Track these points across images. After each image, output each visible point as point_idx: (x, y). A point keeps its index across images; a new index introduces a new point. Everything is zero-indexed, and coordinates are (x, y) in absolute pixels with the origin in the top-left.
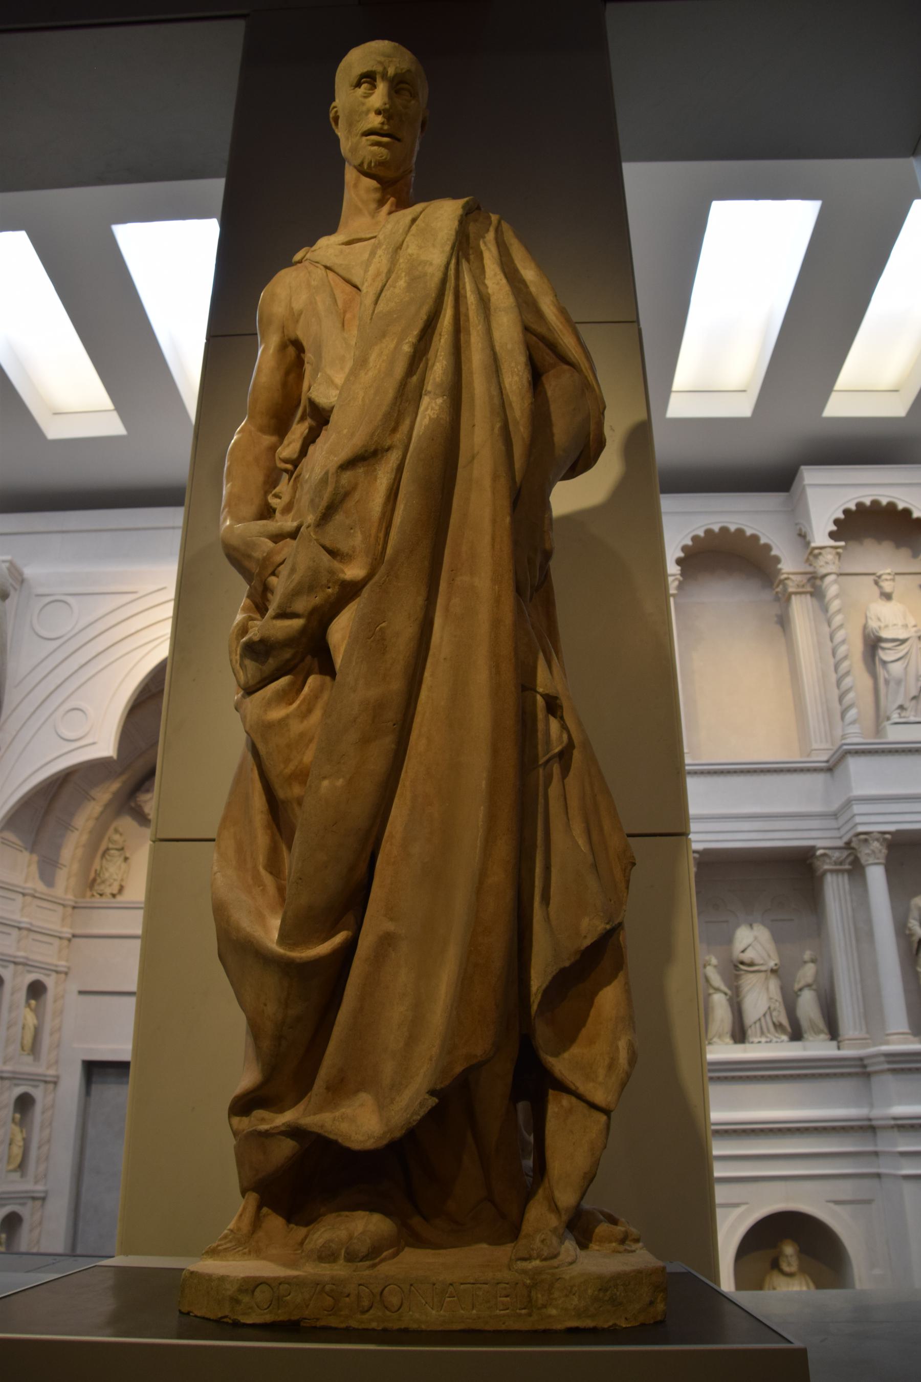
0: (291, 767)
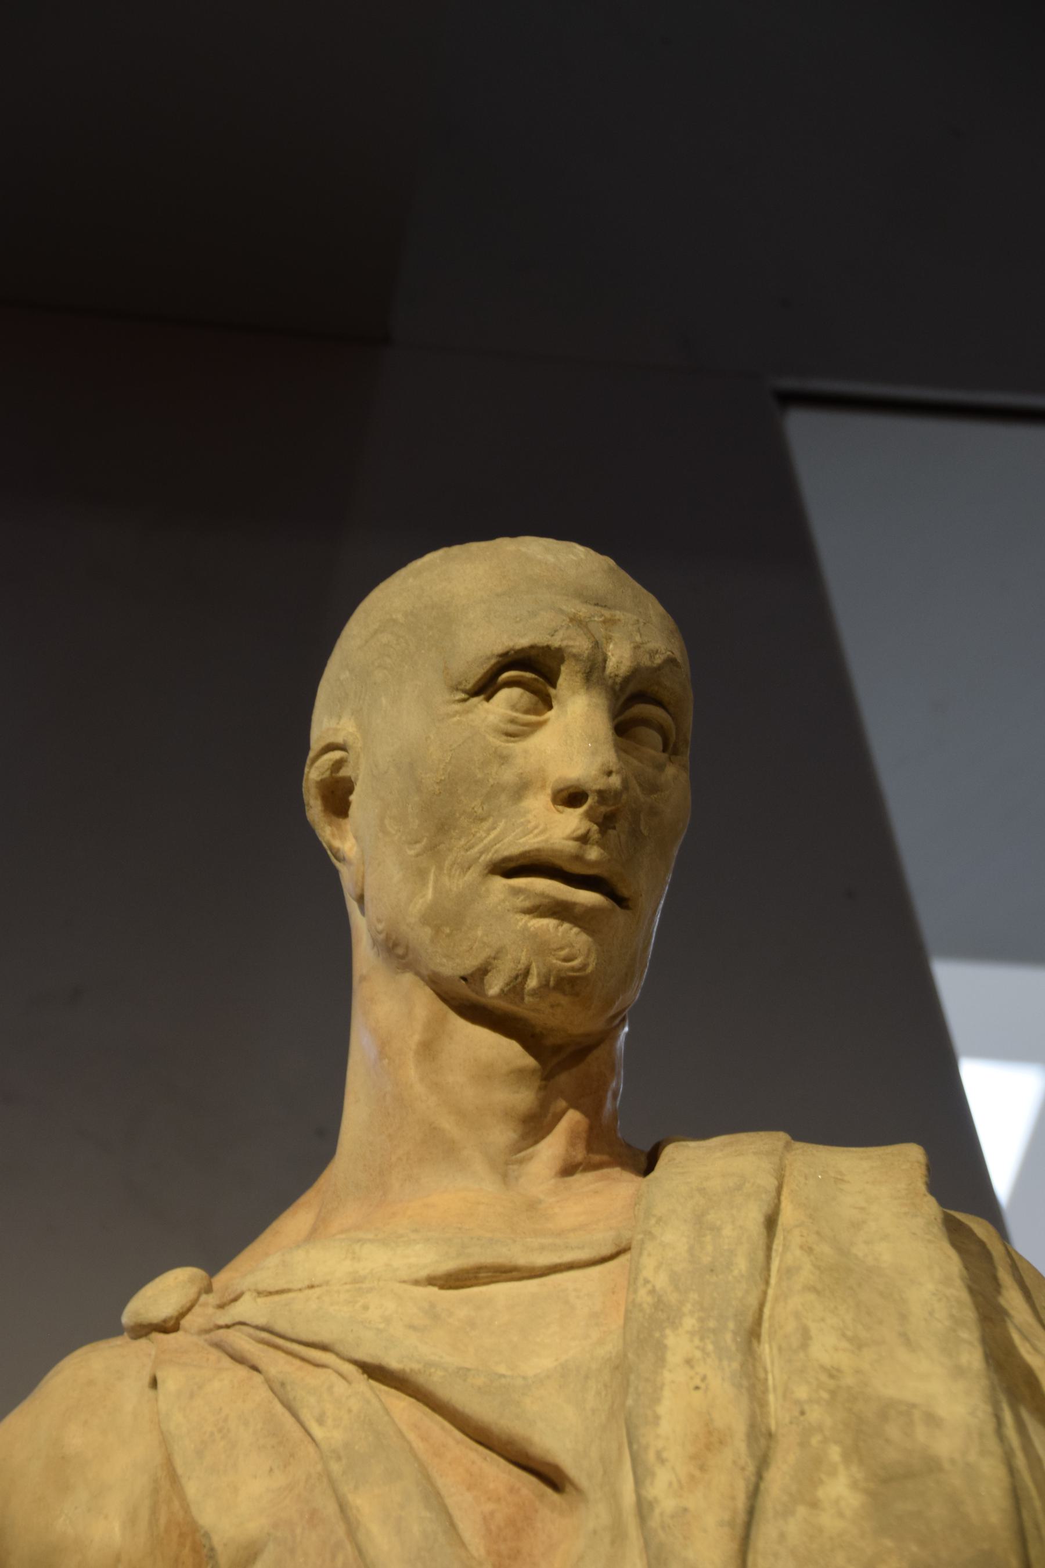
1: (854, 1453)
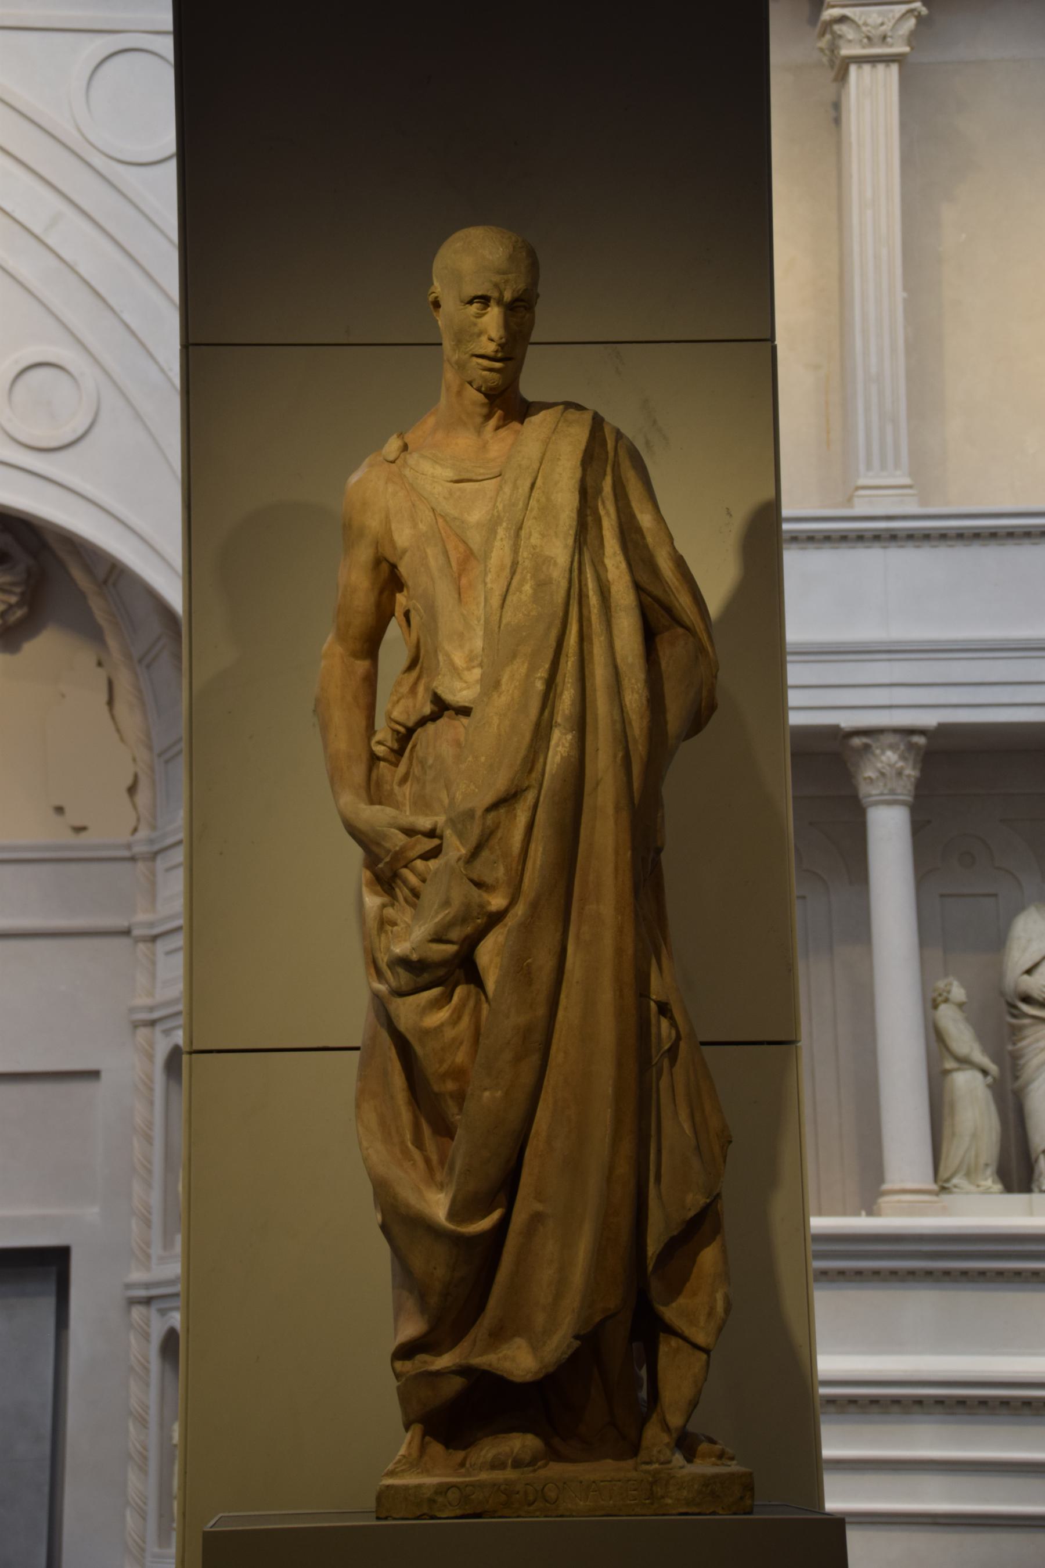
0: (445, 1066)
1: (533, 576)
